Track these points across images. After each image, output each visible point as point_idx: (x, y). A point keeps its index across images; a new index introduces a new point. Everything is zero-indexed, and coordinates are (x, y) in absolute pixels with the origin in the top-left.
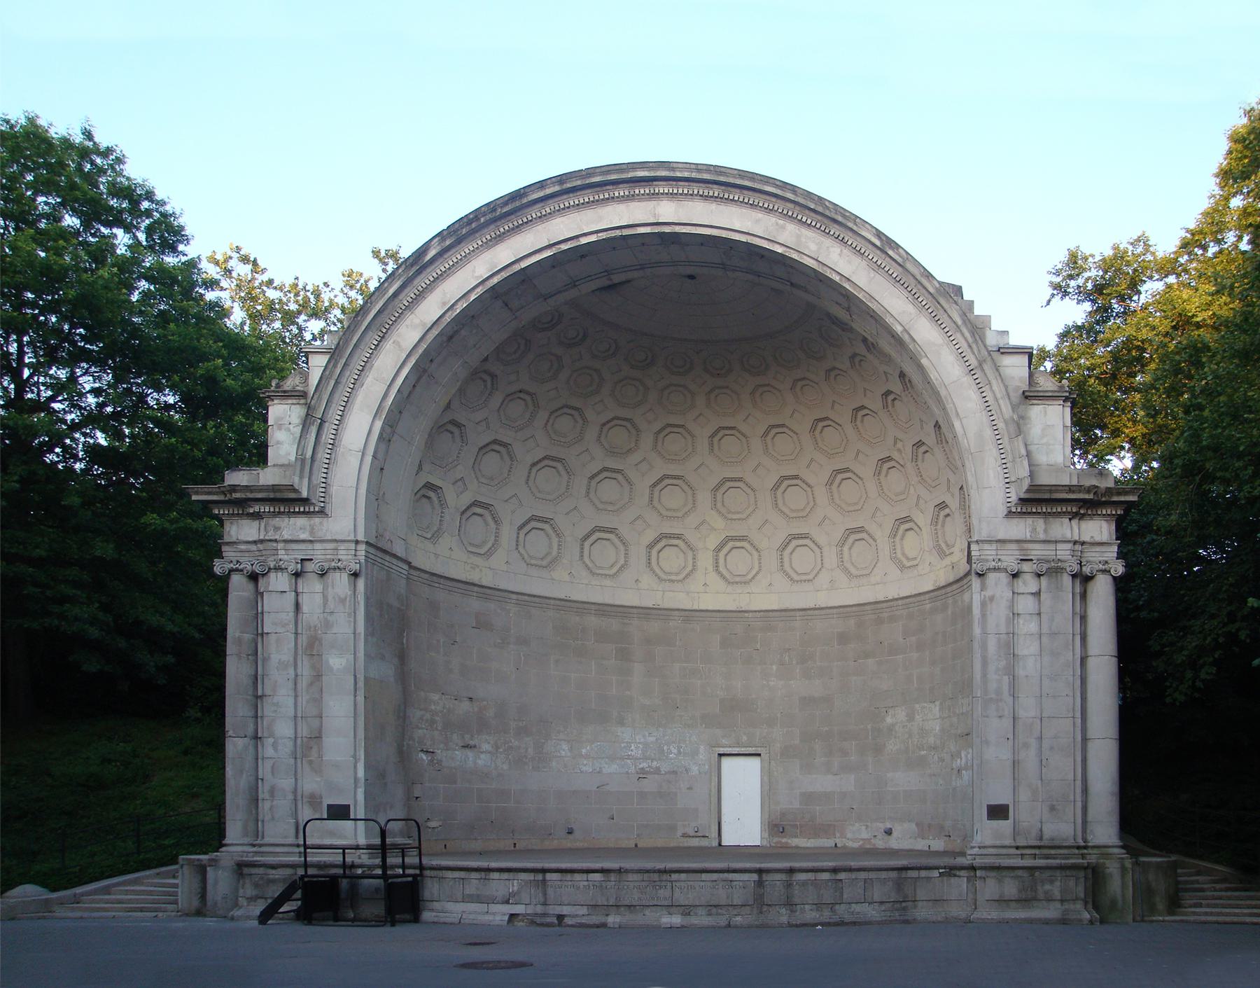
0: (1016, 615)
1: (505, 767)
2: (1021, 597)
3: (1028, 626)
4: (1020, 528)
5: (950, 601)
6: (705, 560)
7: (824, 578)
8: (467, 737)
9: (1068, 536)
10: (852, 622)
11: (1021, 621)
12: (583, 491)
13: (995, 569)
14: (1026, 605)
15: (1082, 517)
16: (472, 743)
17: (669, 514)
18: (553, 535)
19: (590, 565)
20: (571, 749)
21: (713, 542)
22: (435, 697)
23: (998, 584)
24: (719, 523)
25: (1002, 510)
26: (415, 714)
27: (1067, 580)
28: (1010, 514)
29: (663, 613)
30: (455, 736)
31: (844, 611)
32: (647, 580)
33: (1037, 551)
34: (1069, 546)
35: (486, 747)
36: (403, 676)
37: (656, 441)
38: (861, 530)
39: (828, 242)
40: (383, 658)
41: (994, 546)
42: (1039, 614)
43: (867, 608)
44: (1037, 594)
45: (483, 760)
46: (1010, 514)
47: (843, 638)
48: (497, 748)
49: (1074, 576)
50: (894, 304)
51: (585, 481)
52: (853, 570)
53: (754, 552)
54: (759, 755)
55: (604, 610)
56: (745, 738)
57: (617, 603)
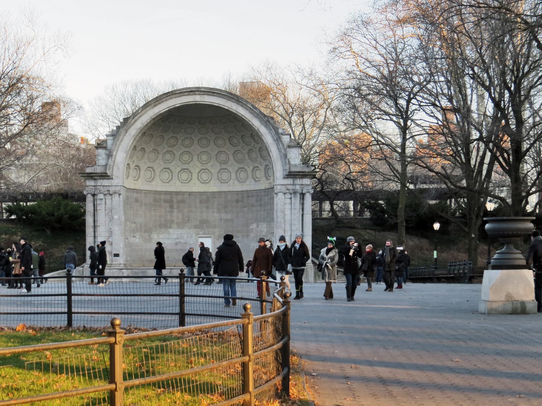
3: (288, 207)
6: (195, 176)
7: (231, 182)
10: (240, 196)
14: (288, 201)
21: (197, 170)
25: (282, 177)
27: (298, 195)
28: (284, 178)
29: (183, 193)
32: (178, 183)
35: (138, 237)
47: (237, 201)
49: (300, 194)
50: (256, 123)
52: (240, 180)
55: (166, 193)
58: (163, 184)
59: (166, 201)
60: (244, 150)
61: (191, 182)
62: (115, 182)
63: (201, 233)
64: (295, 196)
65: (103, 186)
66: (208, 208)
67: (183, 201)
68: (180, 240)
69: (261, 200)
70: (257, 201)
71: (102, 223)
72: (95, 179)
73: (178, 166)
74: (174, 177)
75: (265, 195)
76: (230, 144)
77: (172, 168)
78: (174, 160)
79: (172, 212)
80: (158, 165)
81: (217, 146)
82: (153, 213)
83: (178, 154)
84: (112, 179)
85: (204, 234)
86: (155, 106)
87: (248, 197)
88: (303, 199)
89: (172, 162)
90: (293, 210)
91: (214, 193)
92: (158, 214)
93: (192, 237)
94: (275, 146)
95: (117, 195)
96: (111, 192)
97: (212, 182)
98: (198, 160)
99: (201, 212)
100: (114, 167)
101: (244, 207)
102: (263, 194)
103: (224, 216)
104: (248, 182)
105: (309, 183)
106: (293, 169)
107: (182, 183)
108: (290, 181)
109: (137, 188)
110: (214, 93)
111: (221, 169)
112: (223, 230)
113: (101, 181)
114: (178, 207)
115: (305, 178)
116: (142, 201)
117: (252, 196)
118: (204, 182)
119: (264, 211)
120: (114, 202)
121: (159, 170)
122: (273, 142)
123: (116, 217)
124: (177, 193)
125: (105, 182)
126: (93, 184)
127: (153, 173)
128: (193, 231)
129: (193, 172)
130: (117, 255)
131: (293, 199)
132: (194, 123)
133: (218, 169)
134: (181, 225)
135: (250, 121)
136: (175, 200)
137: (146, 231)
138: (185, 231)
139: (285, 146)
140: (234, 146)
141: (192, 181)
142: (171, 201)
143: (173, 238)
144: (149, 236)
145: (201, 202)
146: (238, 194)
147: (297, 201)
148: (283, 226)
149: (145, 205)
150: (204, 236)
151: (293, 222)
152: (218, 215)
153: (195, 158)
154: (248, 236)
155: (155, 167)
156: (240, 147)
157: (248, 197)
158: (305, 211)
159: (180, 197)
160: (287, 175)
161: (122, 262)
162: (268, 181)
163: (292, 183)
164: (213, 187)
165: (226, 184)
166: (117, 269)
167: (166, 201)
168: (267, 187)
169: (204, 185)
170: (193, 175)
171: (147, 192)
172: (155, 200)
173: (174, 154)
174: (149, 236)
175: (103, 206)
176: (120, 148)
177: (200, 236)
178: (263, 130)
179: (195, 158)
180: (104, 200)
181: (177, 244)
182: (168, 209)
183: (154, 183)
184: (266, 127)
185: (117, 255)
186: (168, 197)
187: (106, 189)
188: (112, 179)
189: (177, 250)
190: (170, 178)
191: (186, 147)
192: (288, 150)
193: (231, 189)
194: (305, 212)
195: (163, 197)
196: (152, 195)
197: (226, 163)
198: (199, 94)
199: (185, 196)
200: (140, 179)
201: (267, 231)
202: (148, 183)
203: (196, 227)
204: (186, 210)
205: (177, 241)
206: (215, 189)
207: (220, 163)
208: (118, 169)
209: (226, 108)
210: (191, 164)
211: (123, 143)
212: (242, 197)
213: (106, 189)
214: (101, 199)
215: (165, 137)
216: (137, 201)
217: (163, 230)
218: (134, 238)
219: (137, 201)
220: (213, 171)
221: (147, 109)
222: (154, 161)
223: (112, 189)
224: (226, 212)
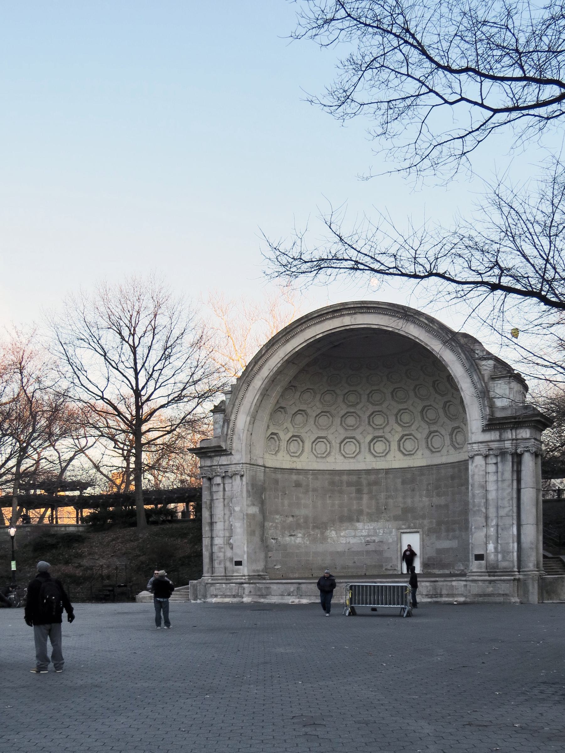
0: (487, 473)
1: (308, 543)
2: (490, 465)
3: (492, 478)
4: (488, 436)
6: (394, 446)
7: (444, 451)
8: (291, 531)
9: (510, 437)
10: (456, 470)
11: (490, 476)
12: (339, 423)
13: (478, 455)
14: (492, 468)
15: (516, 429)
16: (293, 534)
17: (378, 427)
18: (327, 443)
19: (344, 454)
20: (336, 534)
21: (397, 437)
22: (278, 517)
23: (479, 460)
24: (399, 429)
25: (481, 430)
26: (268, 524)
27: (509, 458)
28: (484, 431)
29: (377, 471)
30: (286, 532)
32: (369, 458)
33: (494, 445)
34: (510, 442)
36: (263, 511)
37: (368, 397)
38: (458, 427)
40: (254, 505)
41: (477, 445)
42: (497, 472)
43: (462, 463)
44: (496, 464)
45: (299, 540)
46: (484, 431)
47: (453, 478)
48: (304, 535)
49: (512, 455)
51: (340, 419)
52: (457, 446)
53: (415, 440)
54: (418, 532)
55: (350, 472)
56: (412, 525)
57: (356, 469)
58: (346, 461)
59: (349, 484)
60: (455, 398)
61: (388, 456)
62: (236, 458)
63: (403, 527)
64: (503, 460)
65: (220, 465)
66: (413, 490)
68: (373, 538)
71: (219, 518)
72: (210, 457)
73: (368, 433)
74: (362, 449)
76: (436, 392)
77: (359, 437)
78: (360, 425)
79: (361, 499)
80: (336, 434)
81: (420, 399)
82: (328, 501)
83: (365, 417)
84: (231, 454)
85: (409, 527)
86: (287, 341)
88: (519, 463)
89: (357, 427)
94: (469, 380)
95: (238, 477)
96: (229, 474)
97: (419, 453)
98: (397, 422)
99: (404, 497)
100: (234, 437)
103: (436, 500)
105: (528, 436)
106: (499, 414)
107: (375, 456)
108: (494, 435)
109: (298, 468)
111: (430, 433)
112: (434, 521)
113: (217, 458)
114: (370, 492)
115: (521, 427)
116: (308, 485)
118: (409, 454)
120: (235, 488)
121: (338, 441)
122: (465, 375)
123: (237, 509)
124: (368, 472)
125: (223, 460)
126: (209, 464)
127: (328, 445)
128: (391, 525)
129: (391, 440)
130: (239, 563)
131: (500, 465)
133: (426, 432)
134: (374, 517)
135: (427, 344)
136: (364, 482)
137: (314, 527)
138: (380, 524)
139: (486, 378)
140: (442, 396)
141: (391, 452)
143: (362, 536)
144: (322, 533)
145: (403, 482)
147: (508, 467)
148: (484, 510)
149: (314, 490)
150: (408, 530)
151: (500, 502)
152: (427, 499)
153: (392, 420)
155: (330, 437)
158: (523, 482)
159: (373, 477)
160: (487, 425)
161: (246, 574)
163: (498, 438)
164: (420, 460)
165: (438, 454)
166: (236, 583)
167: (349, 484)
169: (408, 458)
170: (392, 443)
171: (316, 473)
172: (332, 483)
173: (359, 417)
174: (322, 533)
175: (221, 493)
176: (242, 409)
177: (402, 531)
180: (222, 485)
181: (368, 543)
182: (354, 495)
183: (330, 459)
184: (452, 350)
185: (239, 563)
186: (354, 478)
187: (223, 469)
188: (231, 454)
189: (368, 552)
190: (358, 450)
191: (377, 405)
192: (491, 384)
194: (523, 485)
195: (345, 478)
196: (327, 476)
197: (435, 422)
198: (348, 314)
199: (380, 476)
203: (396, 518)
204: (383, 495)
205: (368, 539)
207: (428, 423)
208: (239, 439)
209: (390, 329)
210: (388, 429)
213: (223, 469)
214: (219, 484)
215: (338, 391)
216: (298, 485)
217: (346, 524)
218: (293, 538)
219: (298, 485)
220: (418, 436)
221: (276, 347)
223: (233, 469)
224: (438, 495)
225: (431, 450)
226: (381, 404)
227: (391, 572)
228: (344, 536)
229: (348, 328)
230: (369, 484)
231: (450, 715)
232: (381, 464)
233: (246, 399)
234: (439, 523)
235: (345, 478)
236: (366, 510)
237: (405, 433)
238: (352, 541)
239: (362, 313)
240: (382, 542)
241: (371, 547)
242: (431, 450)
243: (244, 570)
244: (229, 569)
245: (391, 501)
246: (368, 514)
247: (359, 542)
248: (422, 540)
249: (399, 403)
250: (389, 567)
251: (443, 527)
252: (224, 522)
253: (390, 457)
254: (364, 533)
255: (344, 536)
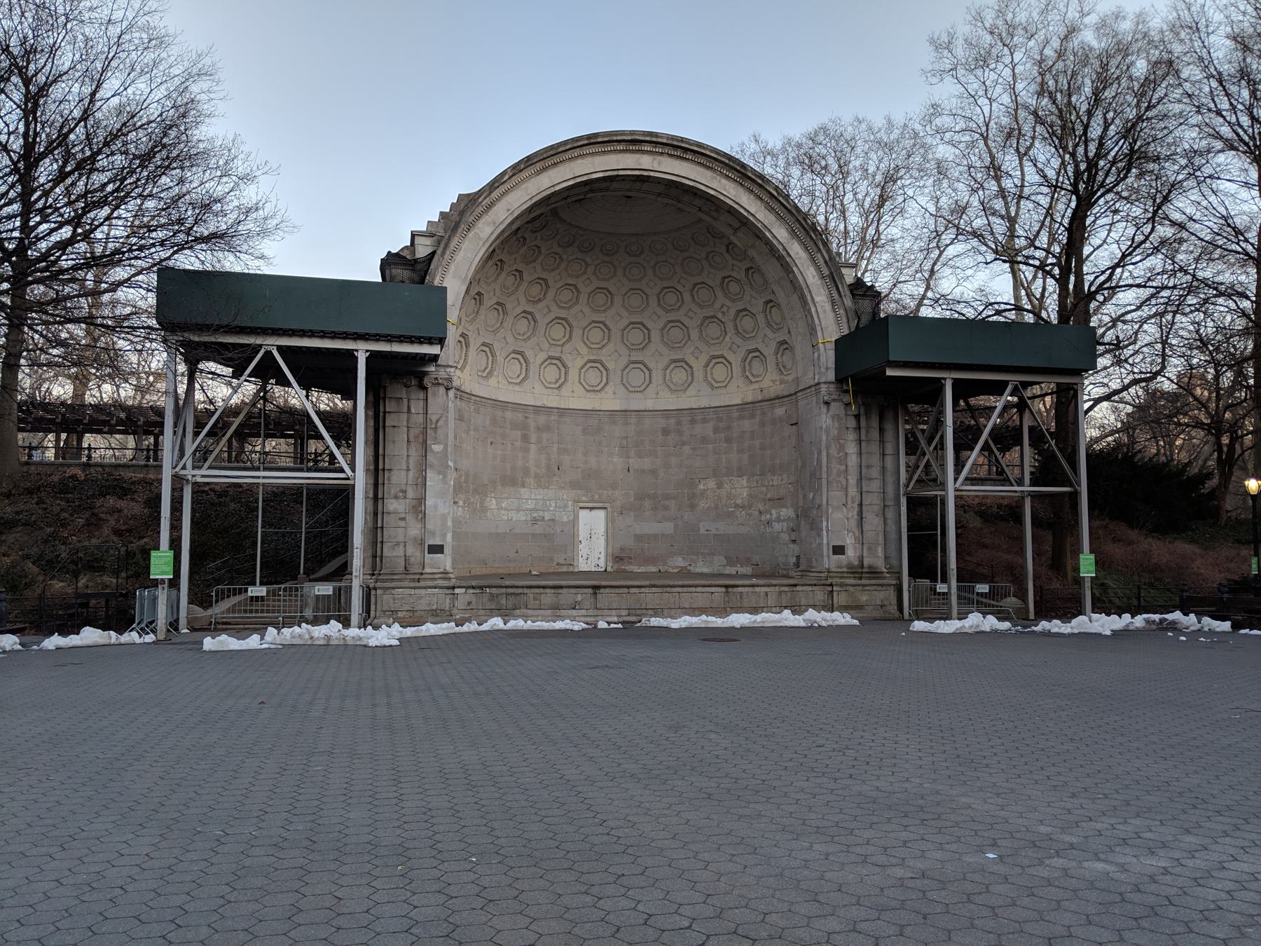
5: (758, 412)
10: (672, 421)
24: (584, 350)
31: (666, 413)
32: (539, 388)
39: (741, 190)
47: (666, 432)
50: (780, 233)
55: (516, 406)
58: (510, 387)
61: (564, 389)
67: (548, 428)
69: (729, 428)
70: (716, 430)
75: (741, 418)
79: (527, 450)
81: (628, 310)
87: (693, 422)
89: (529, 338)
90: (864, 444)
91: (613, 412)
92: (499, 452)
93: (566, 506)
97: (610, 389)
101: (684, 444)
102: (735, 414)
103: (634, 462)
104: (692, 391)
110: (686, 150)
117: (704, 421)
118: (592, 390)
119: (741, 451)
124: (538, 409)
129: (569, 365)
130: (437, 549)
132: (629, 229)
133: (624, 361)
136: (532, 424)
137: (476, 491)
138: (551, 493)
141: (568, 384)
142: (524, 426)
145: (585, 432)
146: (668, 418)
149: (476, 429)
150: (591, 505)
154: (692, 507)
155: (496, 346)
156: (683, 311)
157: (693, 422)
162: (756, 386)
164: (610, 401)
167: (515, 426)
168: (750, 399)
172: (494, 421)
177: (582, 505)
178: (796, 251)
179: (577, 333)
180: (405, 401)
182: (518, 444)
183: (493, 381)
185: (437, 549)
193: (650, 404)
200: (468, 367)
201: (750, 496)
202: (481, 381)
203: (574, 485)
206: (616, 405)
210: (568, 347)
211: (460, 256)
212: (679, 423)
215: (525, 276)
222: (495, 332)
225: (711, 386)
226: (570, 307)
227: (564, 569)
228: (505, 509)
229: (646, 173)
230: (538, 429)
231: (1151, 831)
232: (552, 401)
233: (461, 253)
234: (640, 497)
235: (509, 414)
236: (533, 469)
237: (592, 358)
238: (515, 516)
239: (671, 156)
240: (553, 520)
241: (538, 529)
242: (711, 386)
243: (445, 561)
244: (412, 560)
245: (566, 459)
246: (537, 476)
247: (523, 518)
248: (610, 521)
249: (594, 311)
250: (562, 561)
251: (647, 503)
252: (408, 470)
253: (565, 391)
254: (531, 505)
255: (505, 509)
